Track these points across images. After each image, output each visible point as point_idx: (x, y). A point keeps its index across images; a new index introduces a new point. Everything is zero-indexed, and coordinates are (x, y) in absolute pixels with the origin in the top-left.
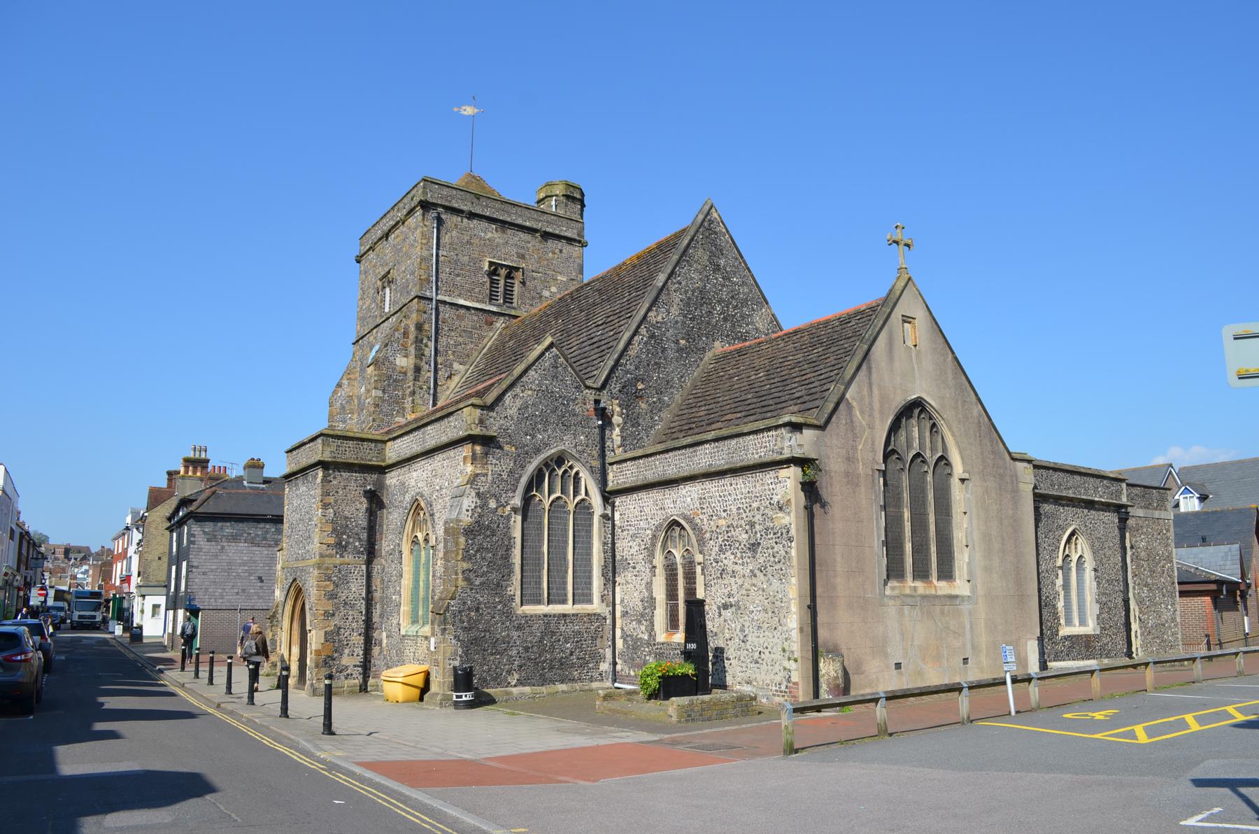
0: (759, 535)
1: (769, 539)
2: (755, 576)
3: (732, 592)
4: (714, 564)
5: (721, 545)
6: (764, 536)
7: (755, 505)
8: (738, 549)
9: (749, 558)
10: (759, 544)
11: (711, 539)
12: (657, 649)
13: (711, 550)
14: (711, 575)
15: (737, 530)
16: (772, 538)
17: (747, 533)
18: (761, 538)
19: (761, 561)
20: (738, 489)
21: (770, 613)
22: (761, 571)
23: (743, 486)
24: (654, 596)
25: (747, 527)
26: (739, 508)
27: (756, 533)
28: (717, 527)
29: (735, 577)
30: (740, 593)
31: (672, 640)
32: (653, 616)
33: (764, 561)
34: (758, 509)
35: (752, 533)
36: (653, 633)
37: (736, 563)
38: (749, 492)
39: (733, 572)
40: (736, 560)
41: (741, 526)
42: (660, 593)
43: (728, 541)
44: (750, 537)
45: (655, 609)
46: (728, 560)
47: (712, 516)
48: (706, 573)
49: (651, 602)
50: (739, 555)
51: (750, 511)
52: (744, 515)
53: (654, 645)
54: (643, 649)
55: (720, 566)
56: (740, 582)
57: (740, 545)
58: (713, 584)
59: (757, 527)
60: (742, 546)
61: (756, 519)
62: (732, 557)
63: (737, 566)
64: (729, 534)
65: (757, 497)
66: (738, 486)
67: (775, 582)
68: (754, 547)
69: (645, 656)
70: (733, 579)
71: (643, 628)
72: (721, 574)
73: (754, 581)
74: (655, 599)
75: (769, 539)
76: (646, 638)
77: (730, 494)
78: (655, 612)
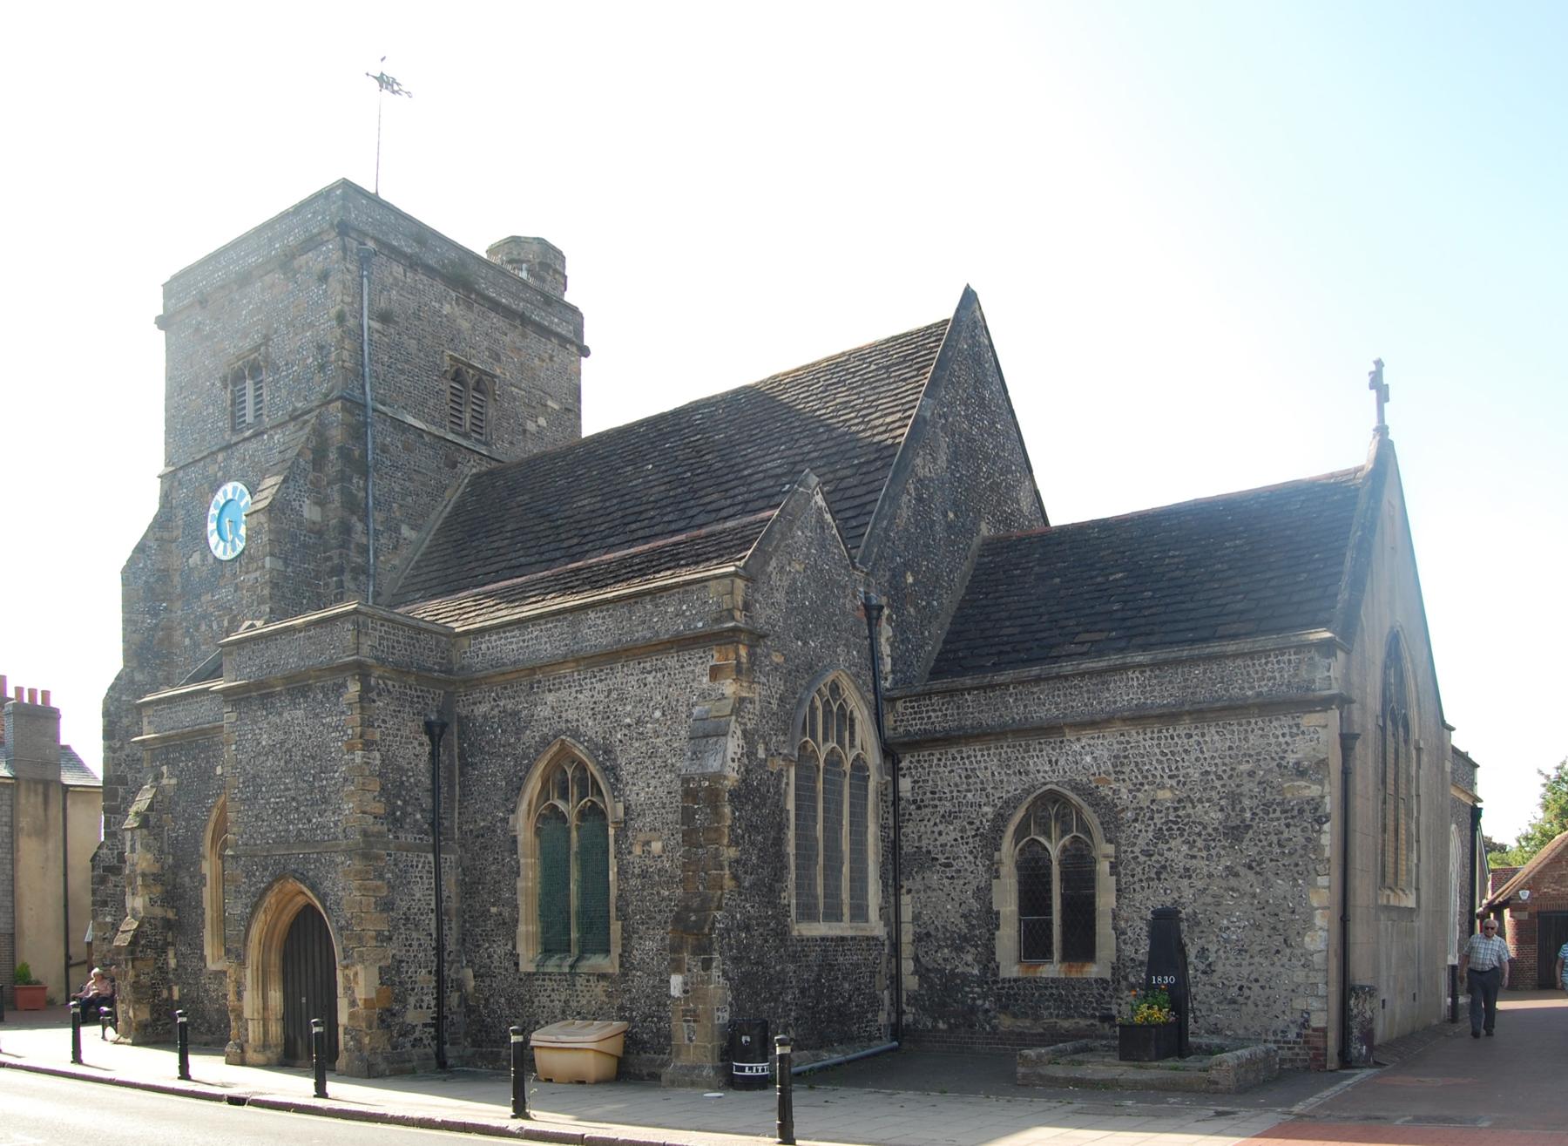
0: (1248, 815)
1: (1272, 820)
2: (1237, 875)
3: (1183, 900)
4: (1142, 858)
5: (1161, 829)
6: (1261, 814)
7: (1244, 767)
8: (1199, 834)
9: (1224, 848)
10: (1249, 827)
11: (1136, 820)
12: (1003, 988)
13: (1136, 837)
14: (1133, 876)
15: (1200, 806)
16: (1278, 819)
17: (1222, 810)
18: (1252, 819)
19: (1253, 852)
20: (1206, 742)
21: (1266, 931)
22: (1251, 868)
23: (1216, 737)
24: (995, 908)
25: (1223, 802)
26: (1207, 773)
27: (1243, 810)
28: (1153, 801)
29: (1190, 877)
30: (1200, 902)
31: (1039, 975)
32: (992, 938)
33: (1259, 853)
34: (1251, 774)
35: (1233, 810)
36: (992, 965)
37: (1194, 857)
38: (1230, 748)
39: (1187, 870)
40: (1194, 852)
41: (1209, 800)
42: (1007, 901)
43: (1176, 823)
44: (1228, 817)
45: (997, 927)
46: (1177, 852)
47: (1142, 784)
48: (1123, 872)
49: (991, 919)
50: (1200, 844)
51: (1231, 777)
52: (1218, 784)
53: (995, 982)
54: (967, 989)
55: (1158, 862)
56: (1200, 884)
57: (1205, 828)
58: (1138, 888)
59: (1246, 802)
60: (1210, 830)
61: (1245, 789)
62: (1185, 847)
63: (1194, 861)
64: (1181, 813)
65: (1251, 756)
66: (1207, 738)
67: (1281, 885)
68: (1235, 833)
69: (974, 999)
70: (1186, 882)
71: (969, 958)
72: (1158, 873)
73: (1233, 882)
74: (998, 913)
75: (1272, 820)
76: (976, 972)
77: (1186, 751)
78: (997, 933)
